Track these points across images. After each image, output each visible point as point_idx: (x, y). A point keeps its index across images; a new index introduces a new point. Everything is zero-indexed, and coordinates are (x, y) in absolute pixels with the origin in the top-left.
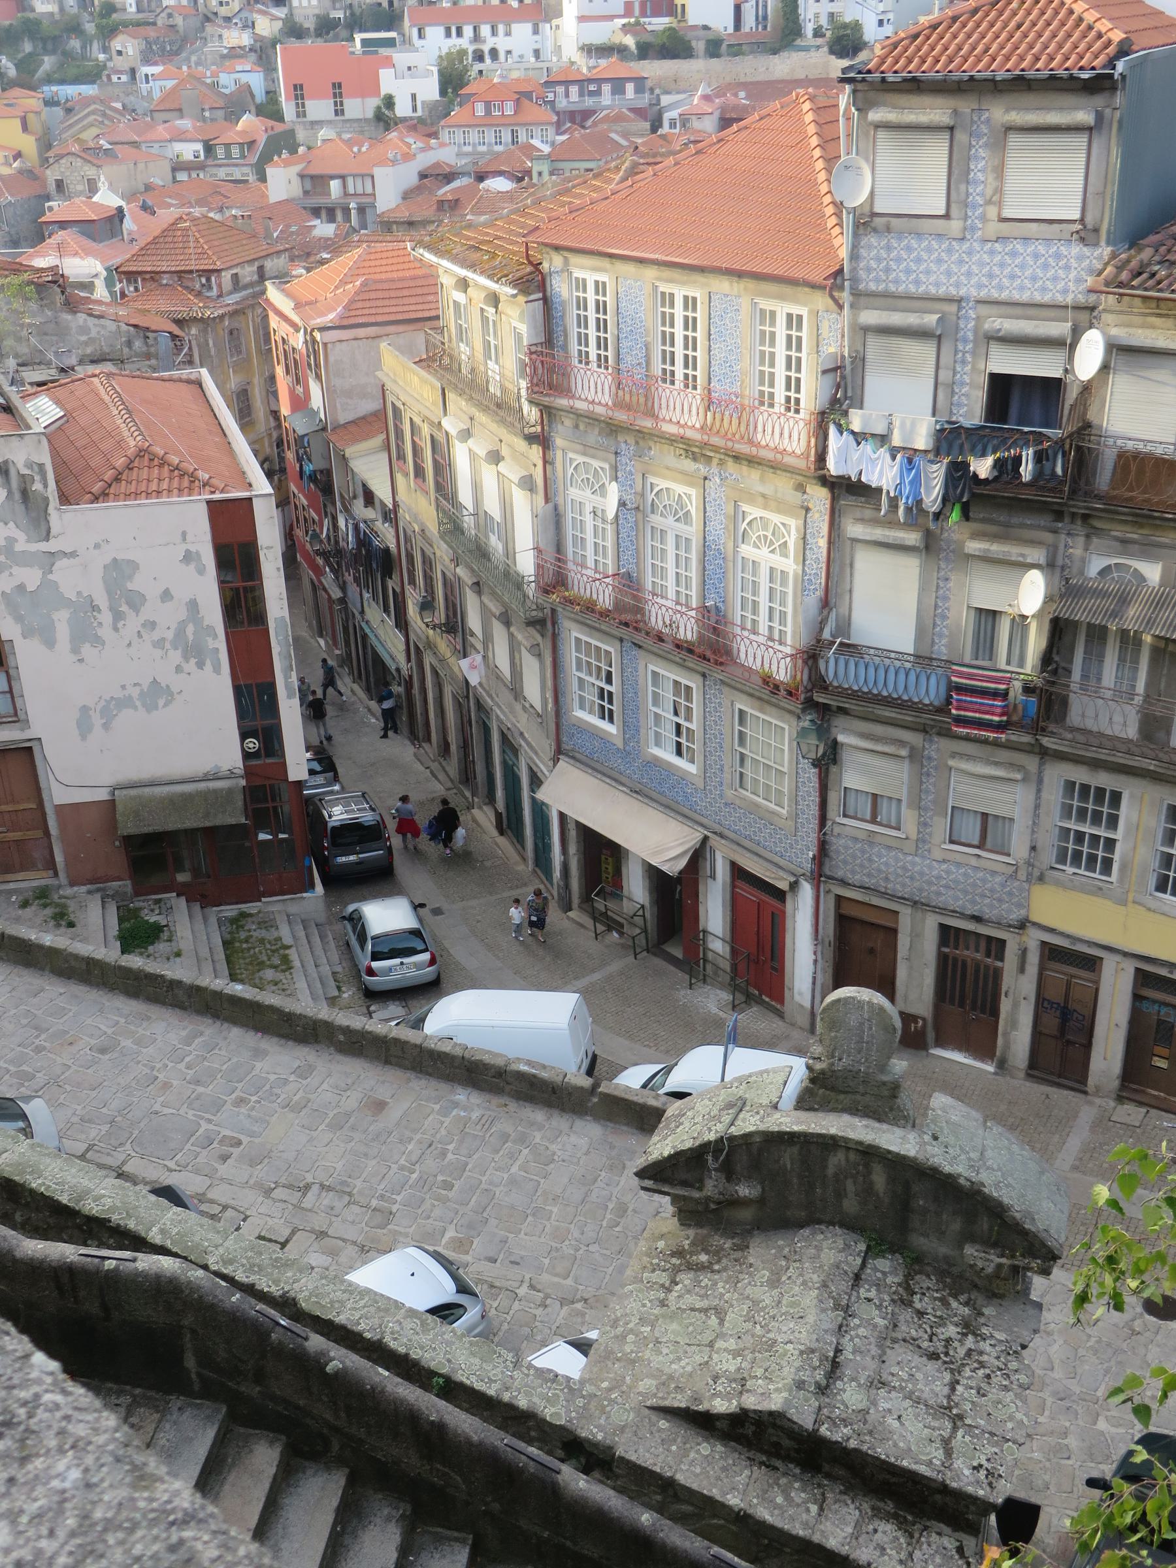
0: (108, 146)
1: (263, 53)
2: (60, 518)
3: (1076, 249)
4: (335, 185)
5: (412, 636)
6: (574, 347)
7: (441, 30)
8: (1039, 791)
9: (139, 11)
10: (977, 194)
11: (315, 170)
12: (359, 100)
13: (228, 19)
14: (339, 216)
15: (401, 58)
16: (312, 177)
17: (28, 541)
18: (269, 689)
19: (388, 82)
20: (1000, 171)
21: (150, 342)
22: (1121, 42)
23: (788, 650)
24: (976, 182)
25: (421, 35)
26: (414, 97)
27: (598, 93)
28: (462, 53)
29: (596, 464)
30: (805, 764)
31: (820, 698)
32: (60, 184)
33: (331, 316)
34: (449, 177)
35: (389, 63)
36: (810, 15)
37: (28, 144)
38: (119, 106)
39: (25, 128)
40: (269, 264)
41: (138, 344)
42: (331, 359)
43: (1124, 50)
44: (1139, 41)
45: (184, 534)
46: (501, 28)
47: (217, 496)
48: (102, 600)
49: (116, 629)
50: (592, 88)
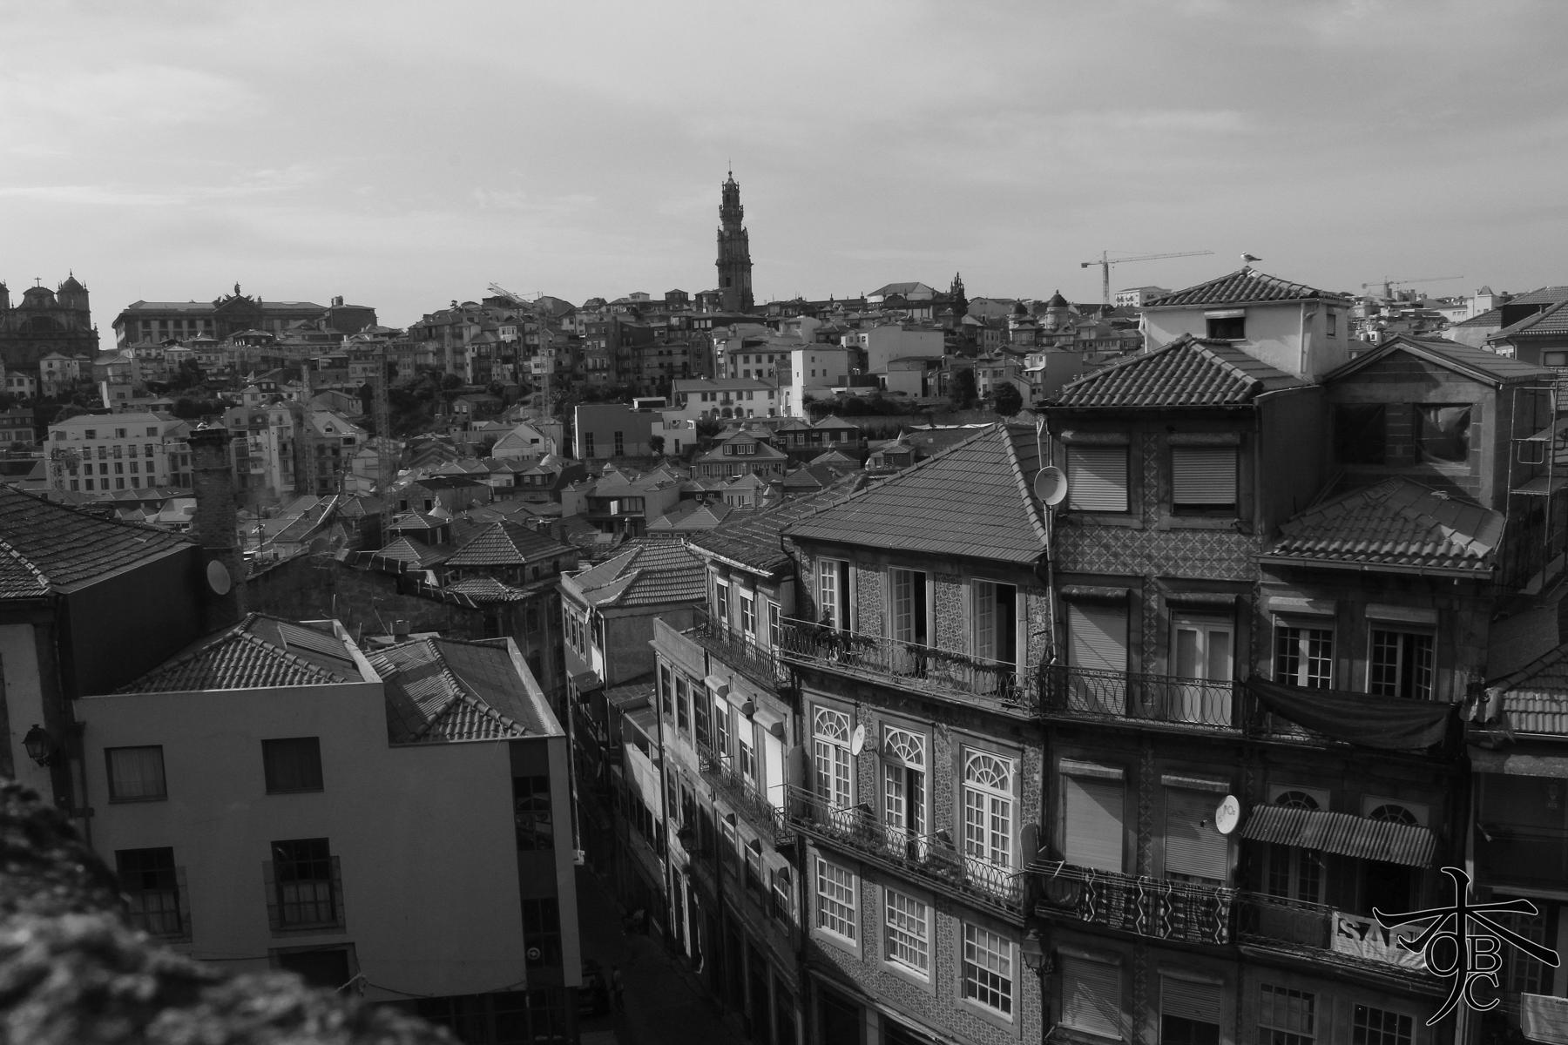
3: (1235, 537)
4: (614, 506)
5: (672, 861)
7: (699, 396)
8: (1239, 995)
10: (1151, 495)
11: (598, 493)
14: (616, 528)
15: (670, 415)
18: (551, 905)
19: (657, 429)
20: (1168, 478)
22: (1254, 385)
23: (1010, 871)
24: (1150, 486)
25: (685, 399)
26: (677, 441)
27: (819, 439)
28: (715, 411)
30: (1028, 972)
31: (1042, 912)
33: (612, 599)
35: (659, 418)
40: (562, 560)
43: (1258, 388)
44: (1267, 385)
50: (815, 435)
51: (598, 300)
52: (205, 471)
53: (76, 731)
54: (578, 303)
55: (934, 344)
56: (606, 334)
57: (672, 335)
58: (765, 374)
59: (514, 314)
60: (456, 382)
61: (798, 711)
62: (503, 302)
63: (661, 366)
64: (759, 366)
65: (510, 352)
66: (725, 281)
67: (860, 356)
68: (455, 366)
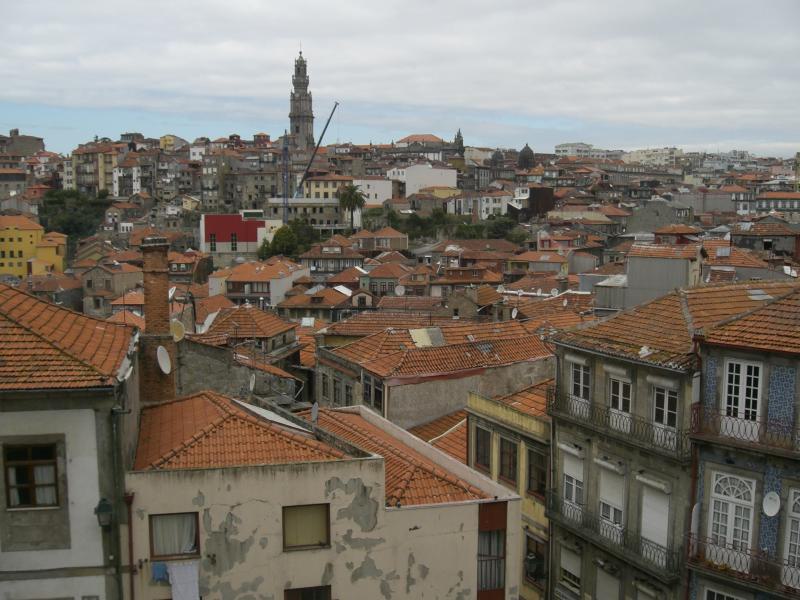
0: (117, 263)
1: (190, 219)
2: (385, 516)
4: (247, 287)
6: (724, 405)
9: (120, 195)
11: (231, 279)
12: (245, 243)
13: (168, 201)
16: (234, 283)
17: (362, 530)
21: (283, 384)
28: (297, 220)
29: (741, 479)
32: (90, 283)
34: (310, 285)
35: (262, 224)
36: (484, 209)
37: (58, 261)
38: (109, 242)
39: (57, 253)
40: (287, 334)
41: (275, 384)
42: (392, 396)
45: (462, 525)
46: (318, 210)
47: (482, 500)
48: (403, 575)
49: (408, 591)
51: (202, 139)
52: (153, 273)
53: (129, 500)
54: (191, 141)
55: (448, 178)
56: (216, 165)
57: (262, 166)
58: (330, 195)
59: (144, 146)
60: (105, 194)
61: (695, 478)
62: (139, 136)
63: (256, 187)
64: (326, 190)
65: (148, 174)
66: (296, 129)
67: (400, 187)
68: (106, 185)
